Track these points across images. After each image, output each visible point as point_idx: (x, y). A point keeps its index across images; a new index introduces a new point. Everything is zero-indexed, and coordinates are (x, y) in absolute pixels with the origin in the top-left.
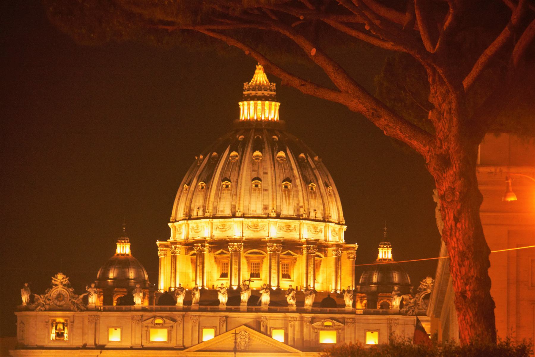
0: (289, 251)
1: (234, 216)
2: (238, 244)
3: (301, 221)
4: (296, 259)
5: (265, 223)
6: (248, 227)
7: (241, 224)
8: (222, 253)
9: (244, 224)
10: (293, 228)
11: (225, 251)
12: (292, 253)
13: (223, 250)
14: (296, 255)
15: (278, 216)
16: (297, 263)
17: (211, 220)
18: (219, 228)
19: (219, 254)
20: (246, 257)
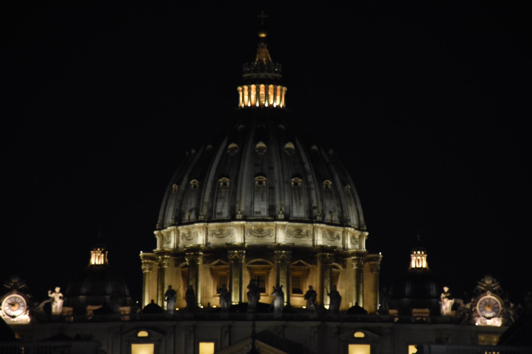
0: (301, 261)
1: (233, 218)
2: (238, 252)
3: (315, 224)
4: (308, 270)
5: (271, 228)
6: (251, 232)
7: (243, 228)
8: (219, 264)
9: (246, 229)
10: (305, 233)
11: (223, 262)
12: (304, 262)
13: (221, 260)
14: (309, 265)
15: (287, 218)
16: (310, 276)
17: (206, 224)
18: (215, 234)
19: (216, 265)
20: (249, 269)
